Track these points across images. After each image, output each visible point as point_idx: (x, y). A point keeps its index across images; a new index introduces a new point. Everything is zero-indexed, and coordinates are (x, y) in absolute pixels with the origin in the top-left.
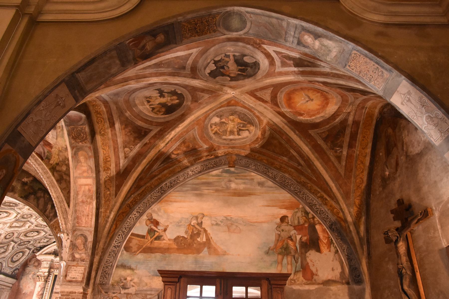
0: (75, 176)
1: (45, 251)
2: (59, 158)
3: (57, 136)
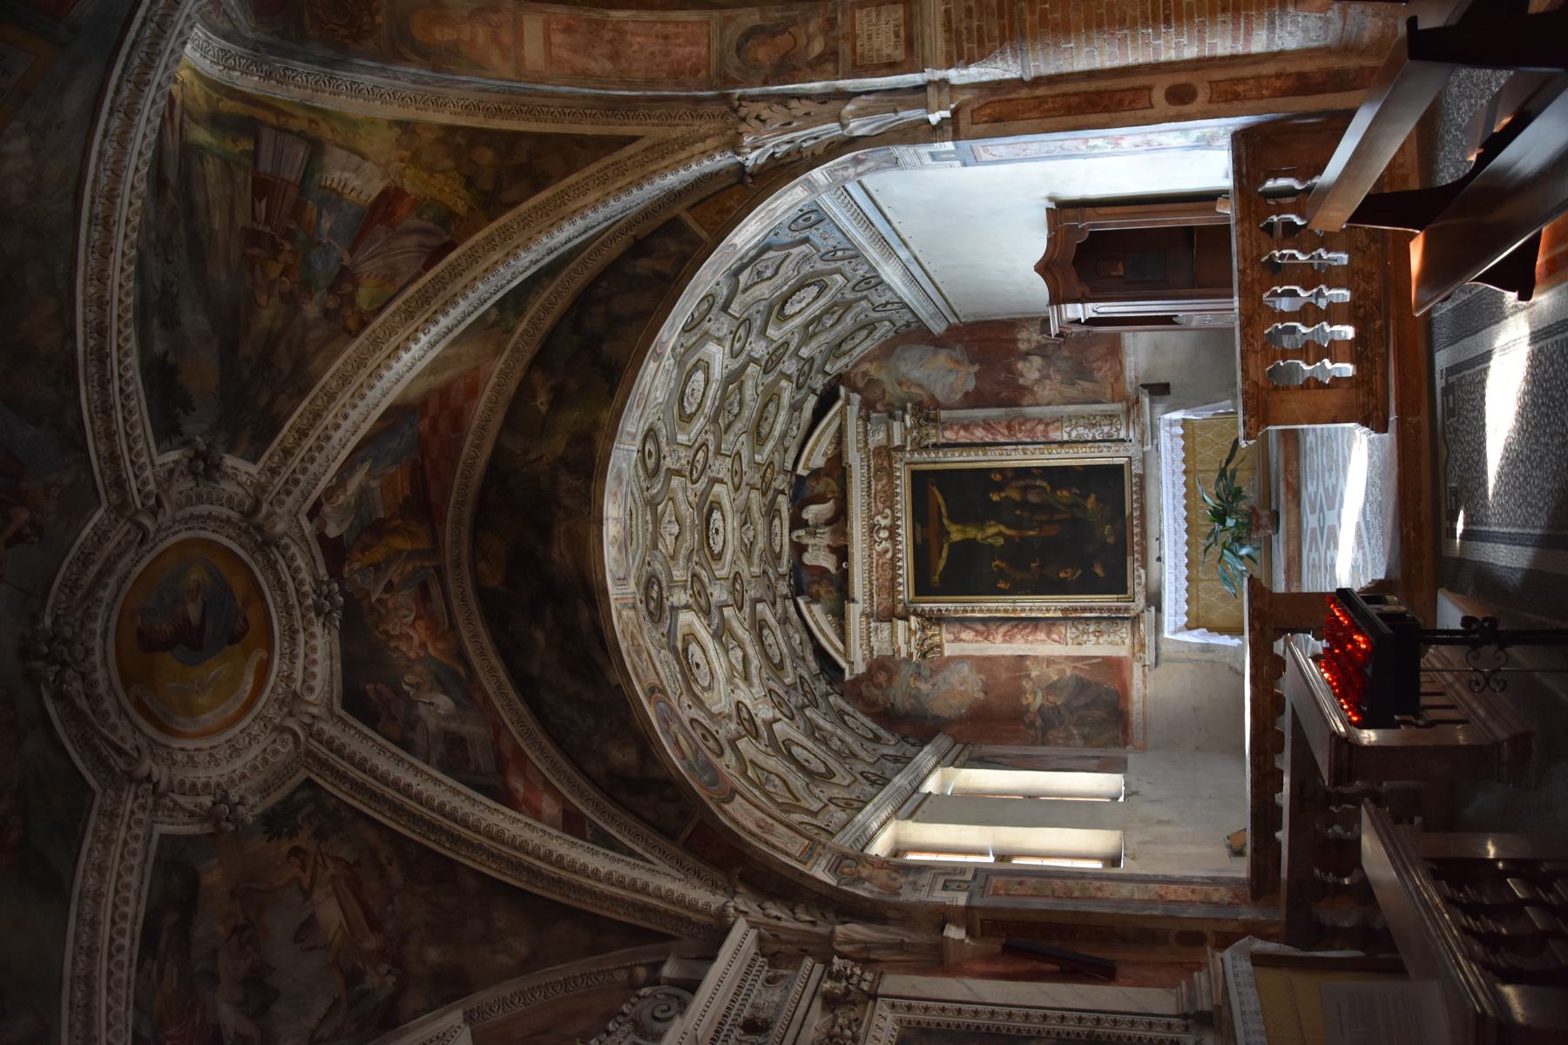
0: (512, 76)
1: (832, 644)
3: (353, 151)
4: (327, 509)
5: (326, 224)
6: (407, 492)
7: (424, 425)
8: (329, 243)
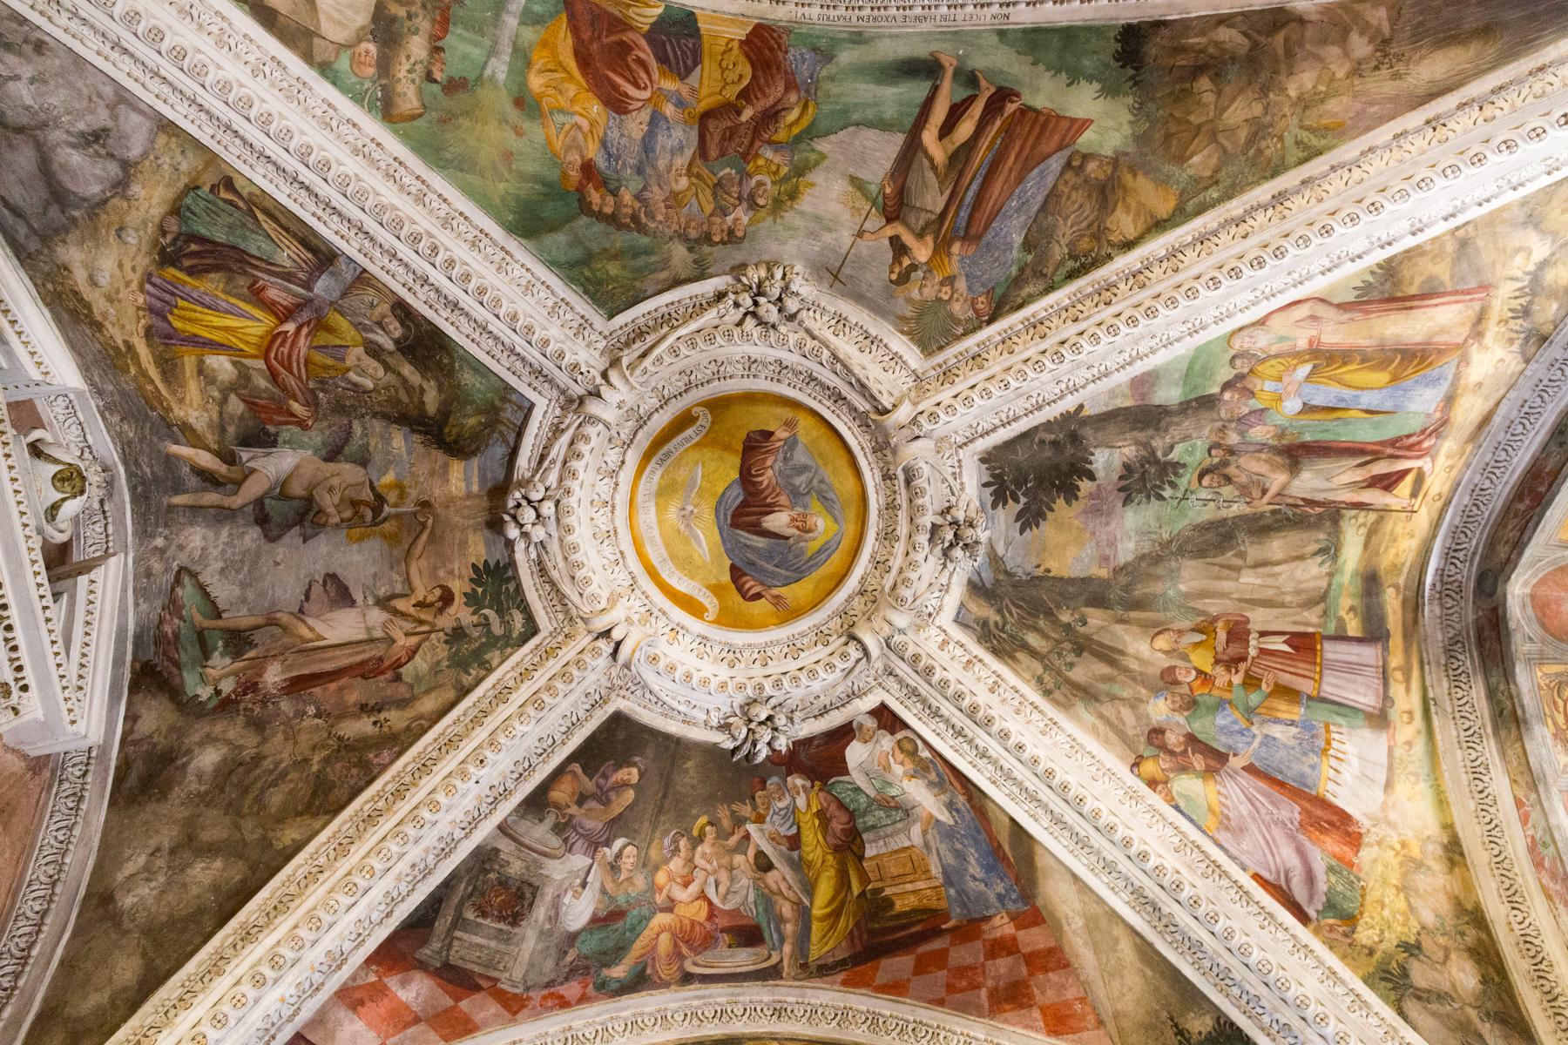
4: (887, 742)
5: (1277, 731)
6: (900, 906)
7: (1002, 926)
8: (1254, 736)
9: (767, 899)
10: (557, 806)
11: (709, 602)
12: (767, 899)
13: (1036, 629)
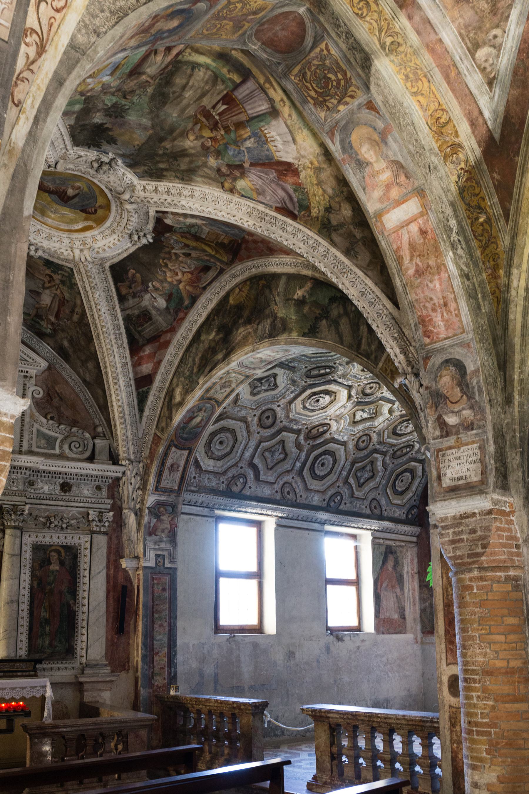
2: (324, 191)
5: (249, 144)
8: (244, 151)
9: (198, 259)
10: (127, 294)
11: (89, 223)
12: (198, 259)
13: (159, 162)
